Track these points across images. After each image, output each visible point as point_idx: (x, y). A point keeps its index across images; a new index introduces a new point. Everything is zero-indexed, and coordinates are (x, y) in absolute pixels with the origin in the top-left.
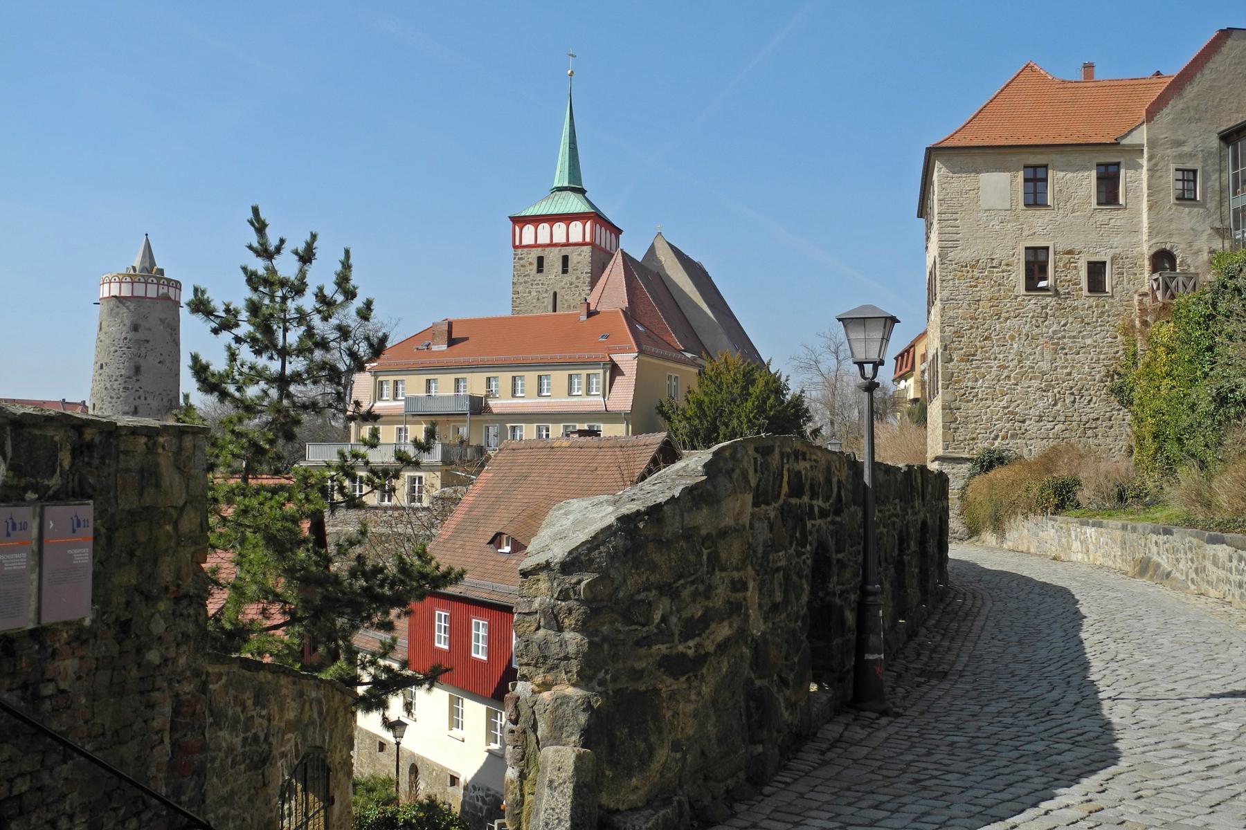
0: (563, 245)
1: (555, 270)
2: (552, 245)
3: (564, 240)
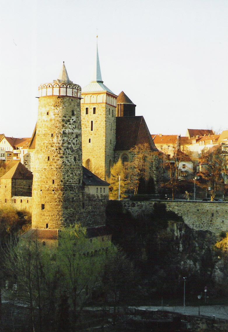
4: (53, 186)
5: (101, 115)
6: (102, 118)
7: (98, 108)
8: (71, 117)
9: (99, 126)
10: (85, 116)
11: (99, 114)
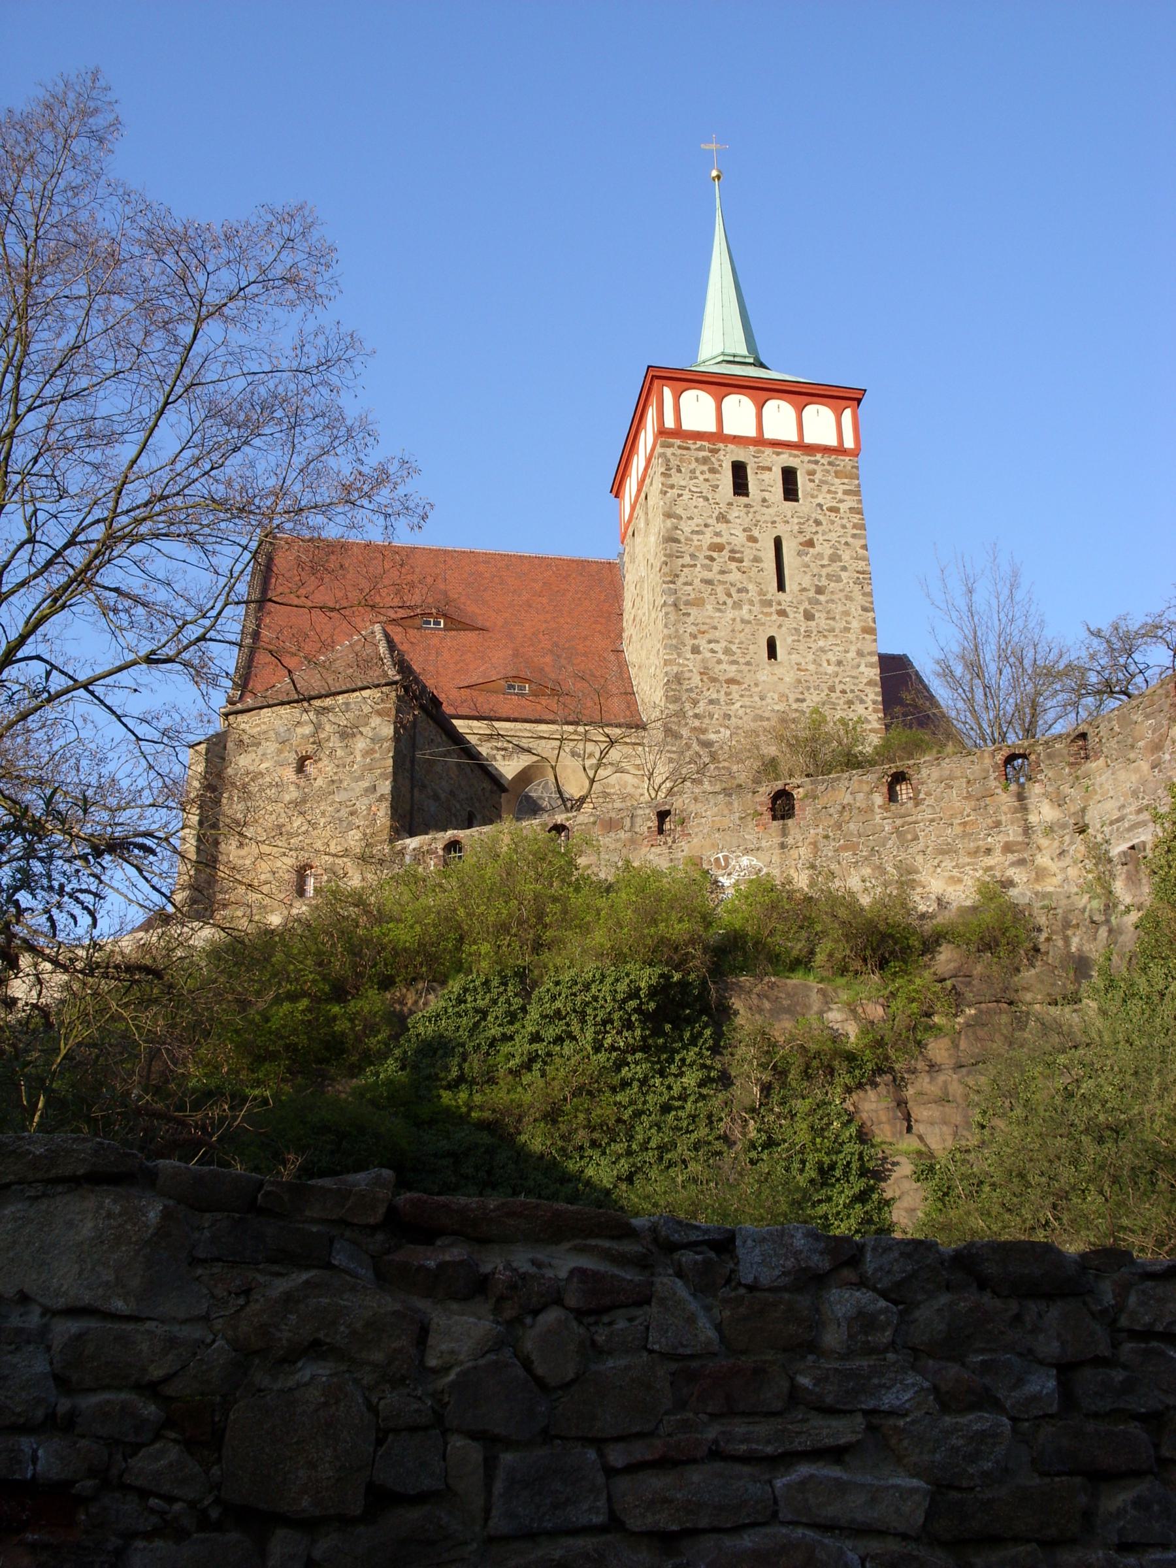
6: (844, 527)
7: (812, 473)
9: (829, 570)
10: (730, 504)
11: (820, 505)
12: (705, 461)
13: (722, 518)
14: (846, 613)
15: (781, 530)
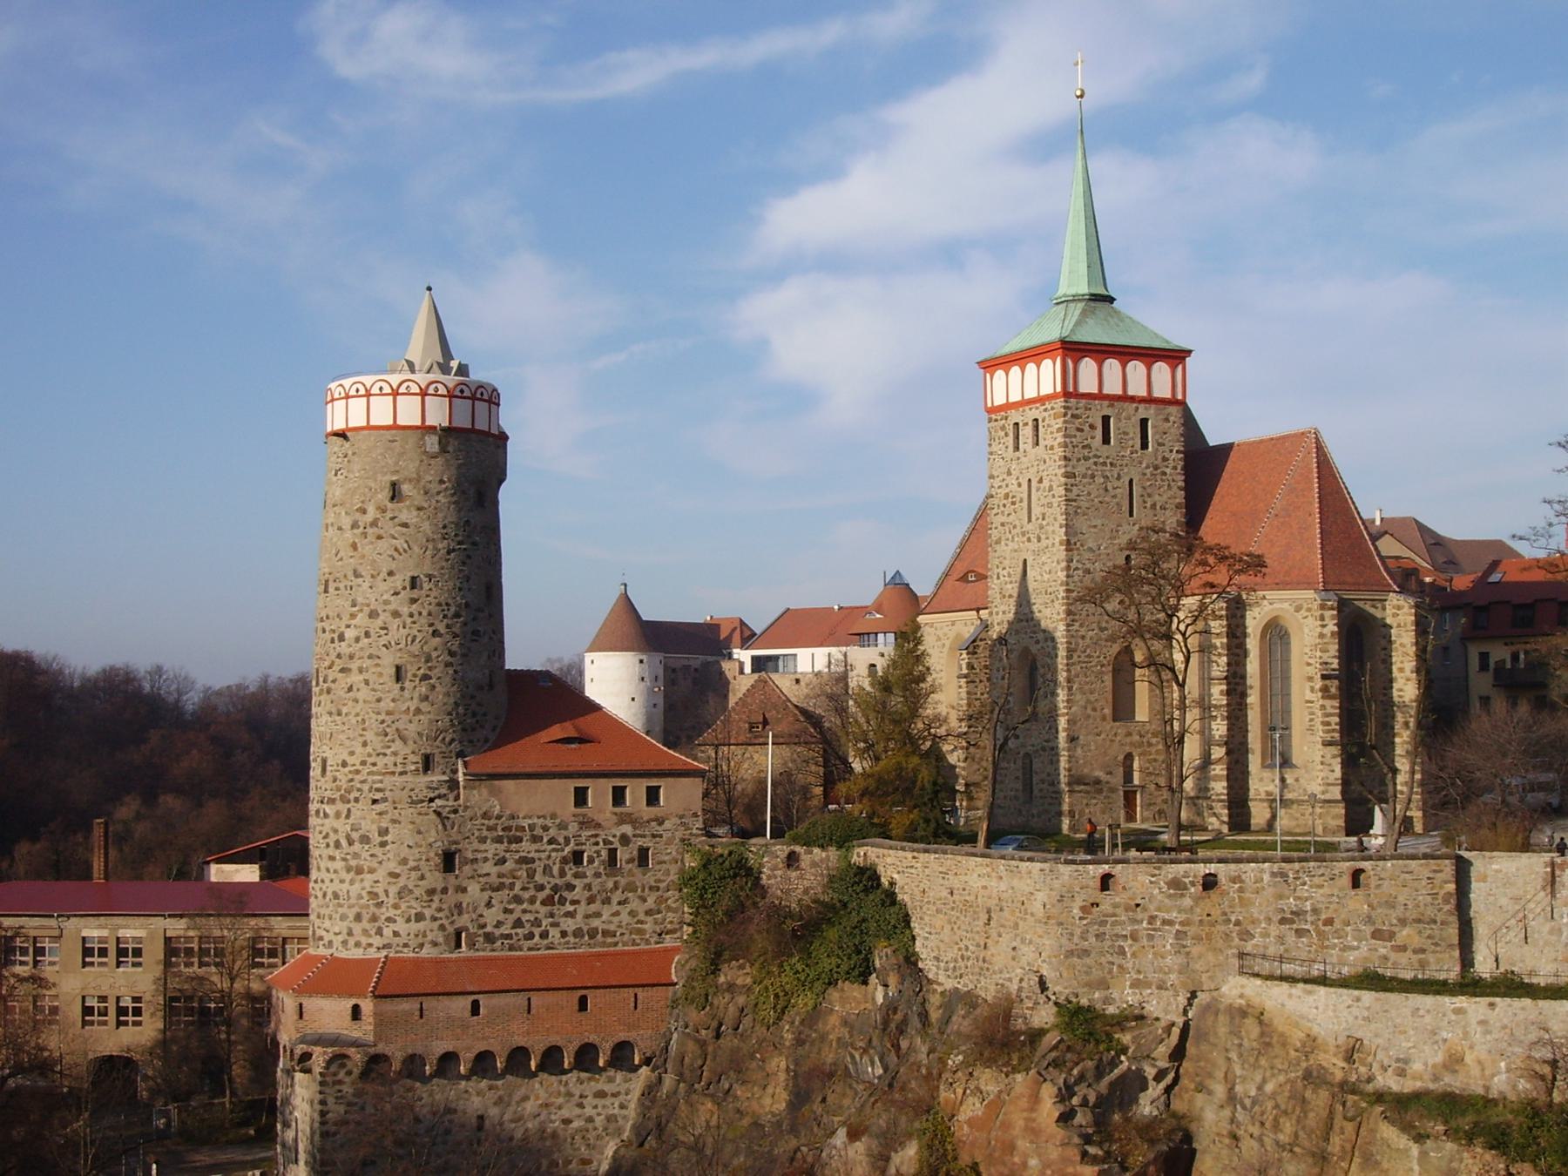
0: (1142, 400)
1: (1131, 443)
2: (1125, 398)
3: (1143, 393)
4: (323, 780)
5: (1052, 448)
8: (384, 511)
12: (1003, 428)
13: (1009, 473)
14: (1053, 532)
15: (1032, 474)
